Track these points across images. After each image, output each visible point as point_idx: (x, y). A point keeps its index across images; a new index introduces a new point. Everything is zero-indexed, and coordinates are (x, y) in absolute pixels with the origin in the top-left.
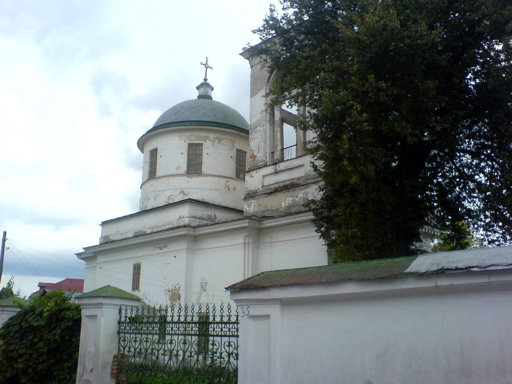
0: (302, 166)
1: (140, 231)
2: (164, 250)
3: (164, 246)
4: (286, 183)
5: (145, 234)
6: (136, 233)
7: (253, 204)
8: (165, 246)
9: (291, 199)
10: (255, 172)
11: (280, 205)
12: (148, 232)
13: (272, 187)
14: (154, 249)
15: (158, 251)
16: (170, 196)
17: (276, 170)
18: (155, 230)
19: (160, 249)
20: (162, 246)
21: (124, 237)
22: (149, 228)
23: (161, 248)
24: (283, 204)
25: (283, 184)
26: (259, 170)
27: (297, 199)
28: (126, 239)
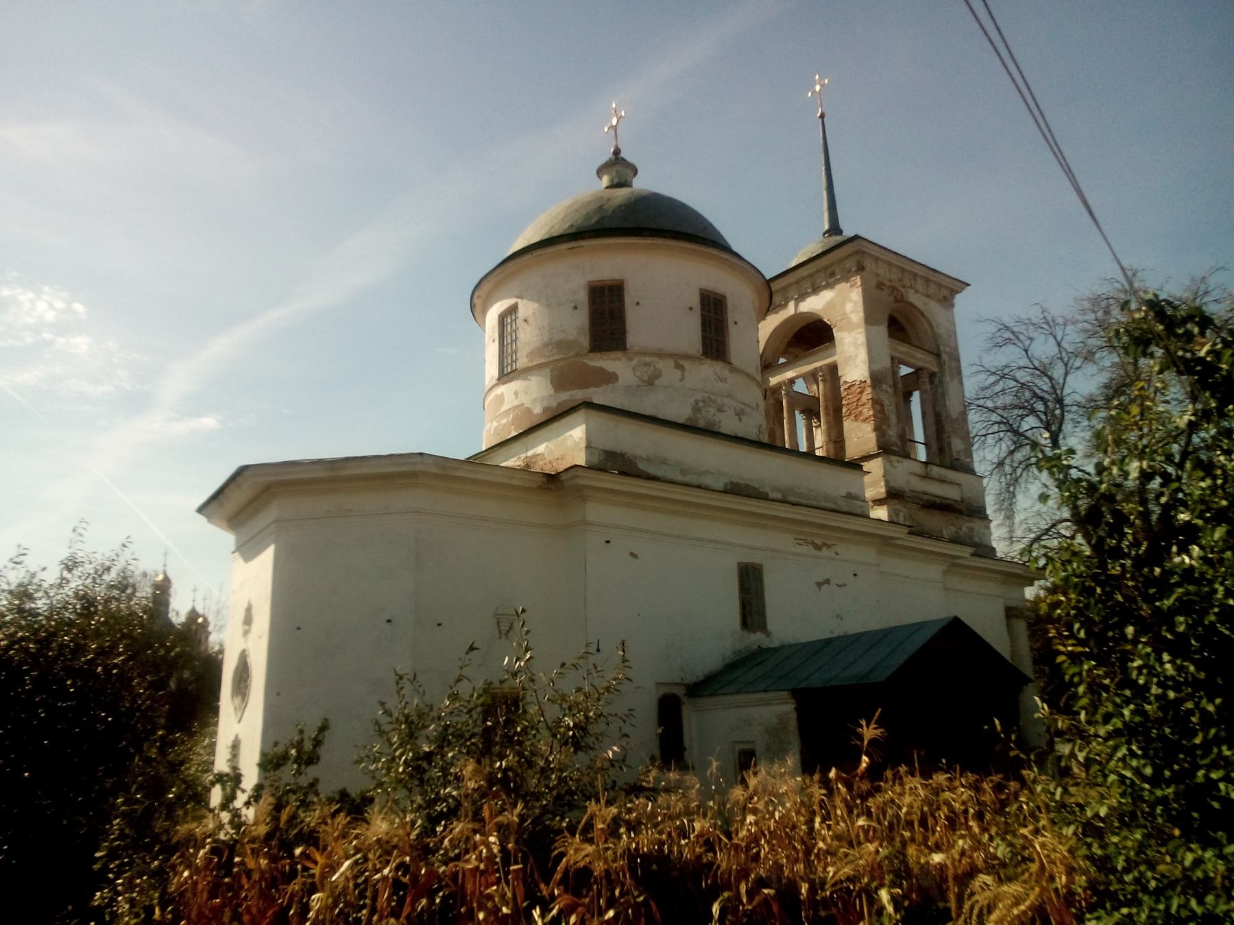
0: (959, 485)
1: (748, 486)
2: (825, 552)
3: (824, 544)
4: (944, 501)
5: (764, 497)
6: (732, 483)
7: (902, 514)
8: (829, 547)
9: (953, 529)
10: (896, 458)
11: (942, 533)
12: (773, 495)
13: (926, 497)
14: (798, 544)
15: (809, 550)
16: (760, 426)
17: (927, 474)
18: (792, 499)
19: (815, 549)
20: (818, 542)
21: (687, 479)
22: (775, 489)
23: (817, 547)
24: (945, 532)
25: (938, 500)
26: (901, 459)
27: (961, 533)
28: (699, 487)
